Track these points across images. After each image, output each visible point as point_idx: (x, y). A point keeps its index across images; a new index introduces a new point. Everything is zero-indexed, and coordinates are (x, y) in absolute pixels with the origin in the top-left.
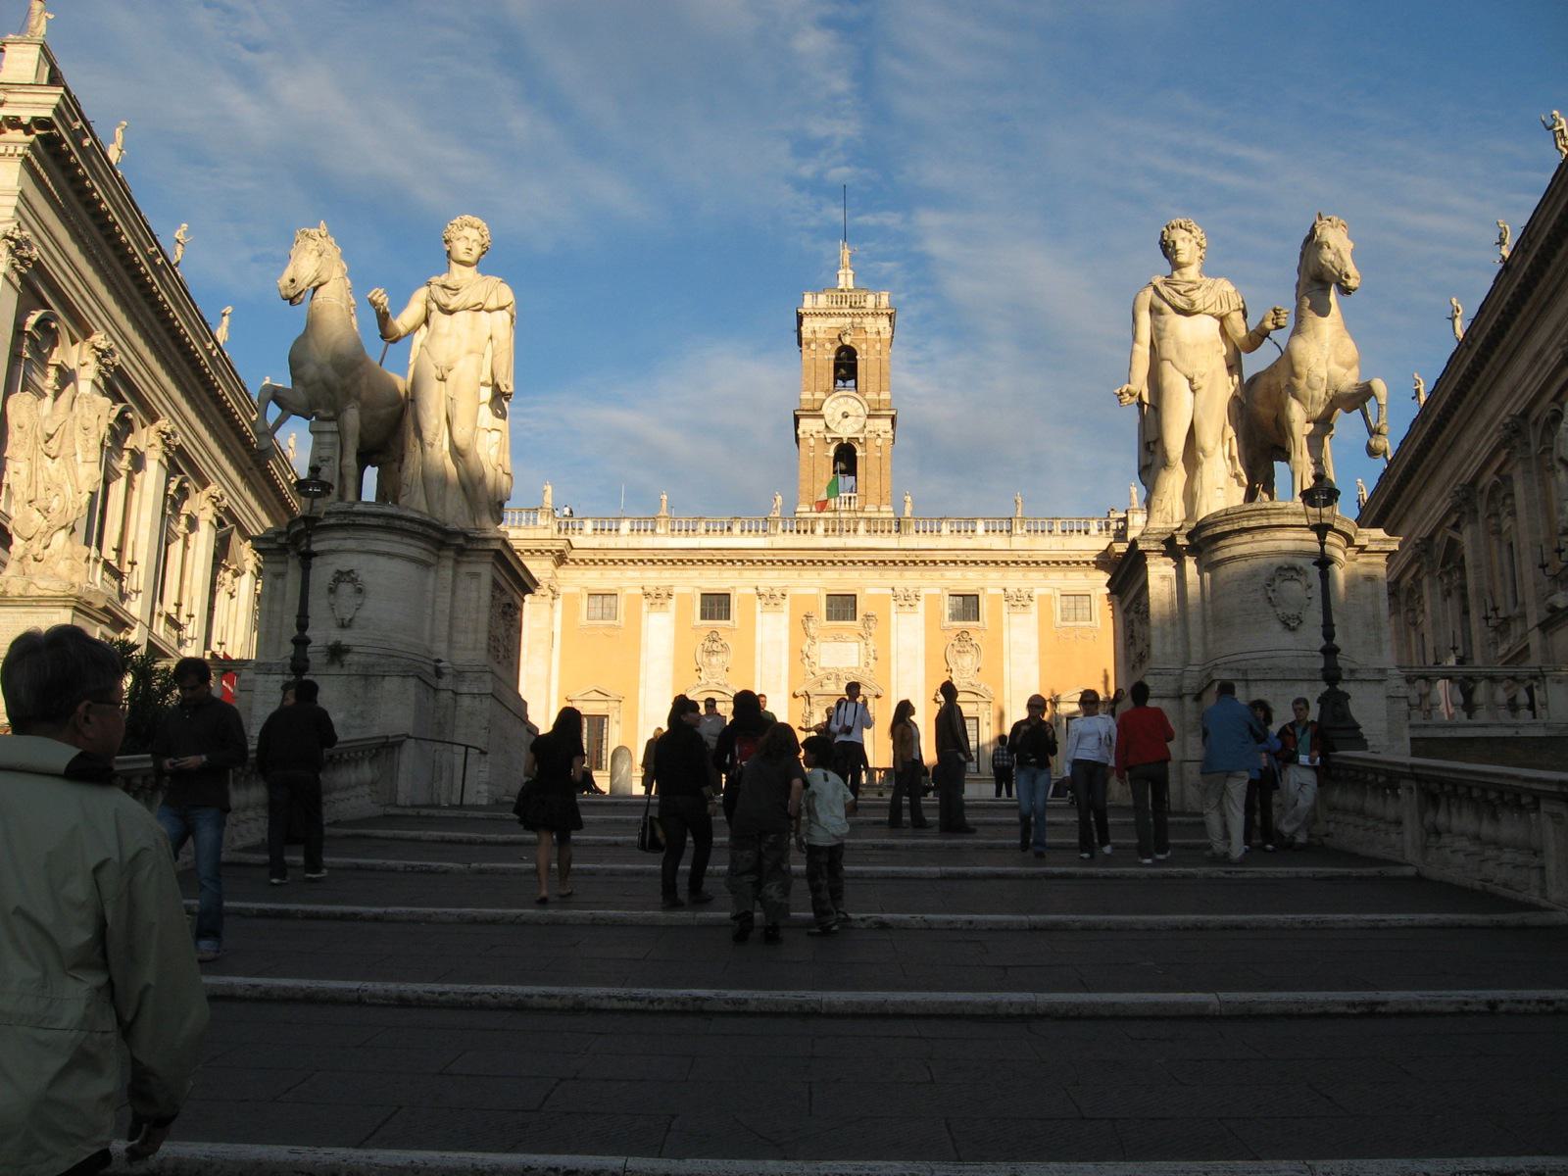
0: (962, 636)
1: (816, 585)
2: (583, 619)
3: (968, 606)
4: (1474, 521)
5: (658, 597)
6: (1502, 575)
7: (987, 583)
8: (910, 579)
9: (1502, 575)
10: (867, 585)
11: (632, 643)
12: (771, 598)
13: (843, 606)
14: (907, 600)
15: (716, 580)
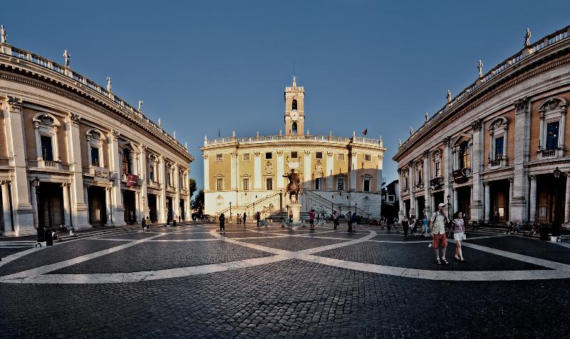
0: (319, 161)
1: (289, 150)
2: (243, 160)
3: (319, 155)
4: (480, 131)
5: (257, 154)
6: (492, 147)
7: (324, 150)
8: (308, 149)
9: (492, 147)
10: (299, 150)
11: (253, 164)
12: (279, 153)
13: (294, 155)
14: (308, 153)
15: (269, 150)
